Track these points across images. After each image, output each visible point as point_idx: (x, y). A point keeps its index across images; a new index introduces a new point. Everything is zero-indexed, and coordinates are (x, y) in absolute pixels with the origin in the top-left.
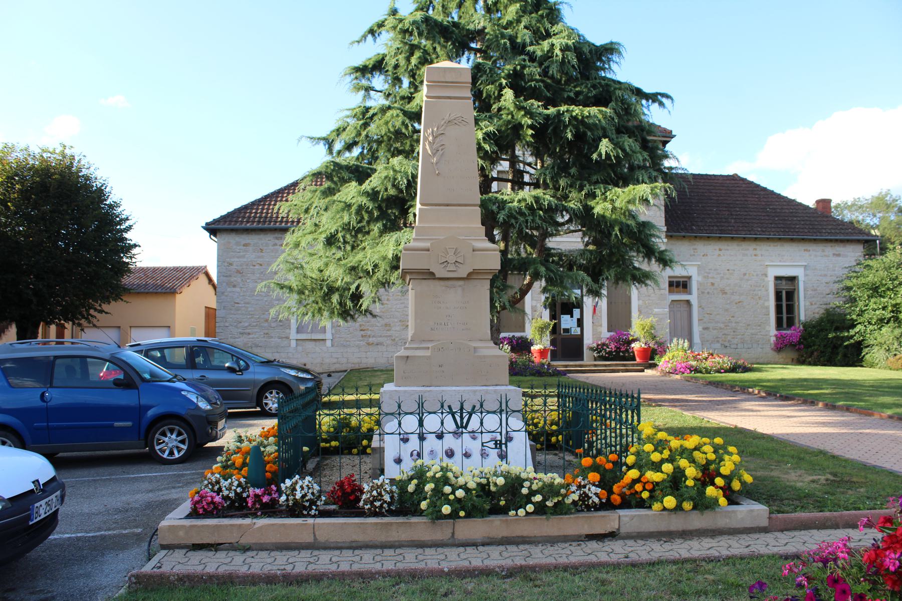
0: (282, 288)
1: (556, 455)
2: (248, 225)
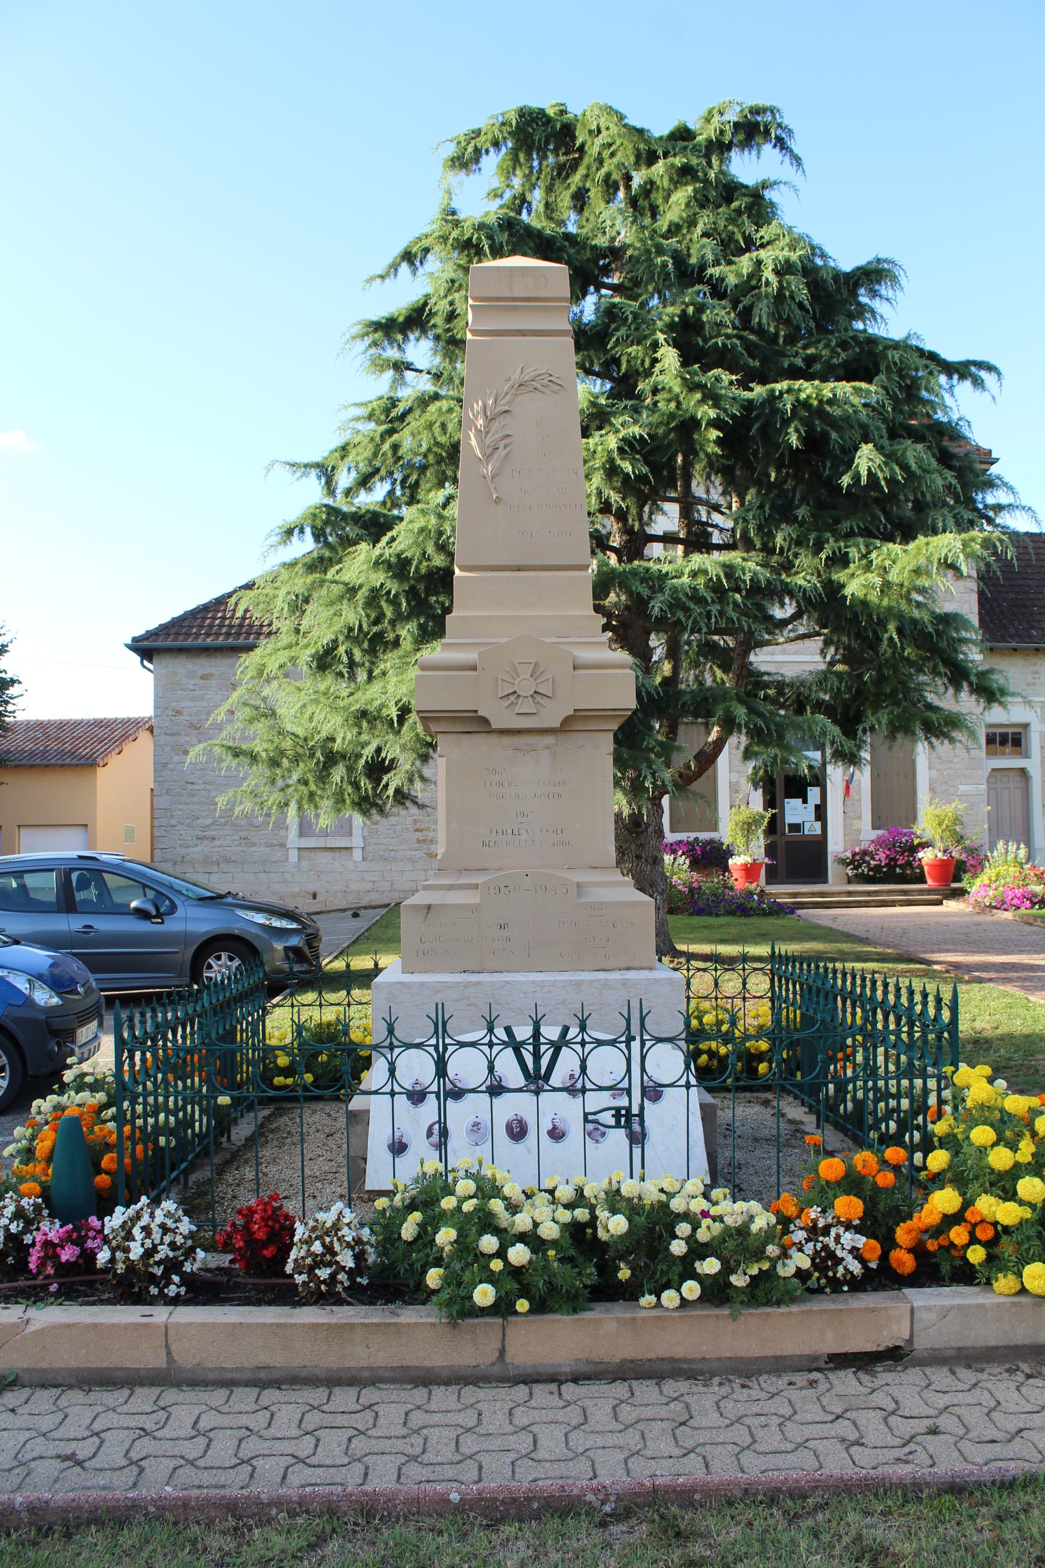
0: (236, 755)
1: (766, 1103)
2: (209, 640)
